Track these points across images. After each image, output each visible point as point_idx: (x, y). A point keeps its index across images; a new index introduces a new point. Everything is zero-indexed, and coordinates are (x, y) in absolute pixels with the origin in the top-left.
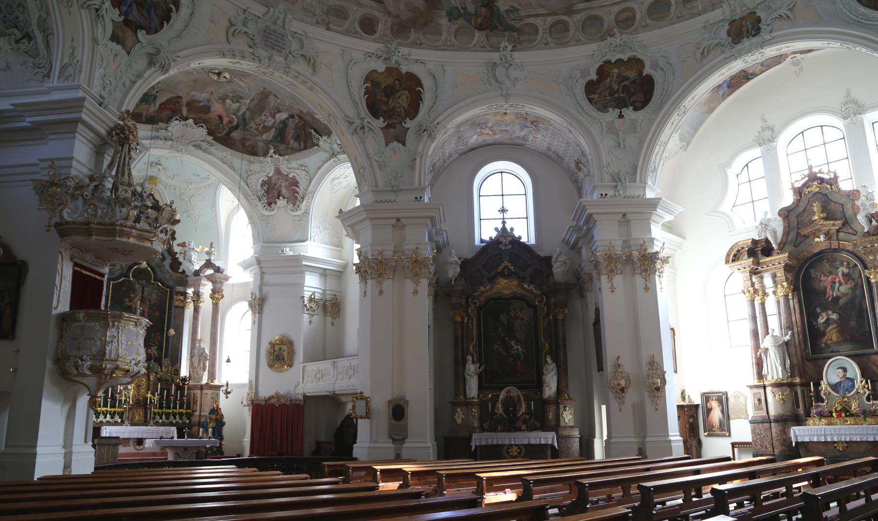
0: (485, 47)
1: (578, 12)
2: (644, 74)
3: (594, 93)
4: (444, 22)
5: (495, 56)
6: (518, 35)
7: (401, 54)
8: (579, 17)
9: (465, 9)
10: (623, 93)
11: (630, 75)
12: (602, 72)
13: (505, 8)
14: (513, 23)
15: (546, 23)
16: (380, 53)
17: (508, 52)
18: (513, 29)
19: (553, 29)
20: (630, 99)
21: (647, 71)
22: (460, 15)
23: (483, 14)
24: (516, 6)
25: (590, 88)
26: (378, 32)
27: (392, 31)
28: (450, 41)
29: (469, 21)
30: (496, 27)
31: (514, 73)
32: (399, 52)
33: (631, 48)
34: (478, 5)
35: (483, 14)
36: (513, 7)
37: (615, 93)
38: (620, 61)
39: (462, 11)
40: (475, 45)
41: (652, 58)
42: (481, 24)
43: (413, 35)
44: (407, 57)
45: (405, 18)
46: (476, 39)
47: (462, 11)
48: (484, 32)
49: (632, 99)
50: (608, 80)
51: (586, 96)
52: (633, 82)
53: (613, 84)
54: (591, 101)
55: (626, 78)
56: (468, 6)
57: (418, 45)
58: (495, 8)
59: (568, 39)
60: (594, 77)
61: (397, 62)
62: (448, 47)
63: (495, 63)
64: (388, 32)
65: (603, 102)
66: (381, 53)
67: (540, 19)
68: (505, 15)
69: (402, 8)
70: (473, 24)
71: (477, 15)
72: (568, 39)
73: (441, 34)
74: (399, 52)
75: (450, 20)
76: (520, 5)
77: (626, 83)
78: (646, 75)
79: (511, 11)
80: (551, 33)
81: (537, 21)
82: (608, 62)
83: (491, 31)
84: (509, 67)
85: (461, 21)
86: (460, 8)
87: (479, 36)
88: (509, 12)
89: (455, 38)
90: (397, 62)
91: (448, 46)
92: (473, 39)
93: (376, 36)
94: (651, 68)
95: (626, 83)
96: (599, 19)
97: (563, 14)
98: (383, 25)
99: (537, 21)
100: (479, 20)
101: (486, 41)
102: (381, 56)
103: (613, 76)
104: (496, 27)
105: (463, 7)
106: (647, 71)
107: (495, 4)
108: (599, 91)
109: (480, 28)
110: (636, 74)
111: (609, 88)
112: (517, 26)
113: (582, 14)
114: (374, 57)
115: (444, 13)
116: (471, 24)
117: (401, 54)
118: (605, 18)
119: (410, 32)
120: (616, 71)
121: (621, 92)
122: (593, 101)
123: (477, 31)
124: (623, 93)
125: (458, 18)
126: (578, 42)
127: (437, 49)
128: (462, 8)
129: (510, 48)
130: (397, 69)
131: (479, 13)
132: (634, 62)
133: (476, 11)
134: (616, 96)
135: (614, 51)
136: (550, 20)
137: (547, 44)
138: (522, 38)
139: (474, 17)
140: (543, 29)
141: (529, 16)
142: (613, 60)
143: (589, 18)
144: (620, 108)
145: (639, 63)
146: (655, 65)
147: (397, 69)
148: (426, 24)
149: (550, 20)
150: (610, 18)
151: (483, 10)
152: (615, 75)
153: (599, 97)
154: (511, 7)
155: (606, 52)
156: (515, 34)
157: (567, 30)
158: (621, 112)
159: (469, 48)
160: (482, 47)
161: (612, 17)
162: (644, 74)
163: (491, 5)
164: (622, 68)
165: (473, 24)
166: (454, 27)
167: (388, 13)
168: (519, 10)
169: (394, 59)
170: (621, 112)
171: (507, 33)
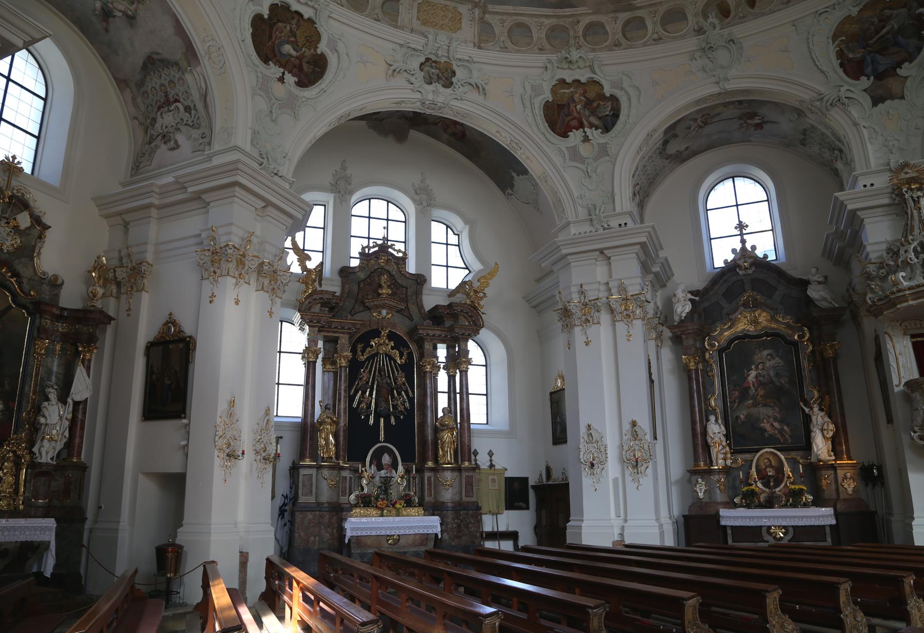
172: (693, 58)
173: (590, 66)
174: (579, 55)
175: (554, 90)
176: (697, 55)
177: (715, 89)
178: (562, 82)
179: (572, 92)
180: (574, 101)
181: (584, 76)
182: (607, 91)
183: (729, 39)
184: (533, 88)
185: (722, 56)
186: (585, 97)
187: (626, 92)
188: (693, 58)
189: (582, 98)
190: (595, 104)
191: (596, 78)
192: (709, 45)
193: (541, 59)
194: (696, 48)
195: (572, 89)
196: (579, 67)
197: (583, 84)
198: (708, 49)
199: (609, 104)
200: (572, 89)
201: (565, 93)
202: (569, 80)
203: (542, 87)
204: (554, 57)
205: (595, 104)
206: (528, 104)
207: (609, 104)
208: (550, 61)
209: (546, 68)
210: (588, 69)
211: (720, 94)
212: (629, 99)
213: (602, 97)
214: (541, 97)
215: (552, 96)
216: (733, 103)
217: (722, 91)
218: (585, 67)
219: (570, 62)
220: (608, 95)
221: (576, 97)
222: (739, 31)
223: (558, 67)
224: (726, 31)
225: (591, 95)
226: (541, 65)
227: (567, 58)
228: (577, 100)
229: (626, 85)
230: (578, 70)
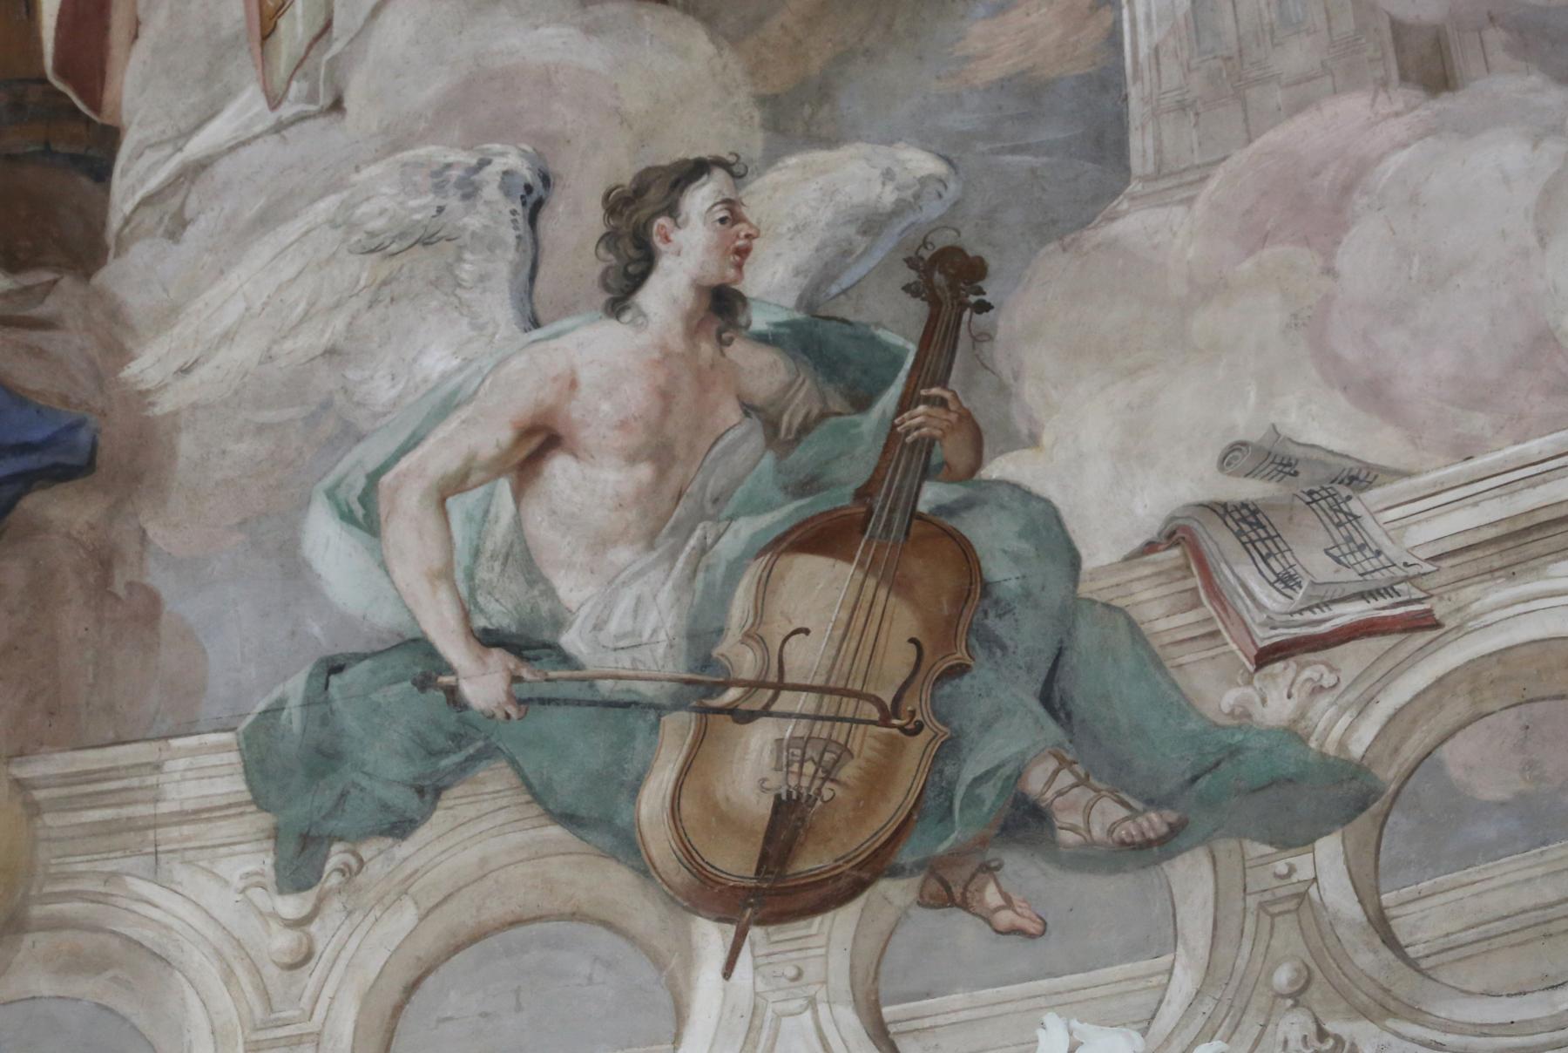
6: (1366, 886)
23: (806, 659)
34: (745, 531)
35: (806, 659)
56: (573, 589)
70: (659, 843)
86: (454, 649)
88: (1220, 541)
105: (498, 613)
107: (997, 468)
123: (711, 937)
125: (430, 792)
128: (489, 639)
131: (747, 663)
139: (677, 729)
154: (1234, 456)
163: (932, 495)
165: (659, 843)
168: (1359, 478)
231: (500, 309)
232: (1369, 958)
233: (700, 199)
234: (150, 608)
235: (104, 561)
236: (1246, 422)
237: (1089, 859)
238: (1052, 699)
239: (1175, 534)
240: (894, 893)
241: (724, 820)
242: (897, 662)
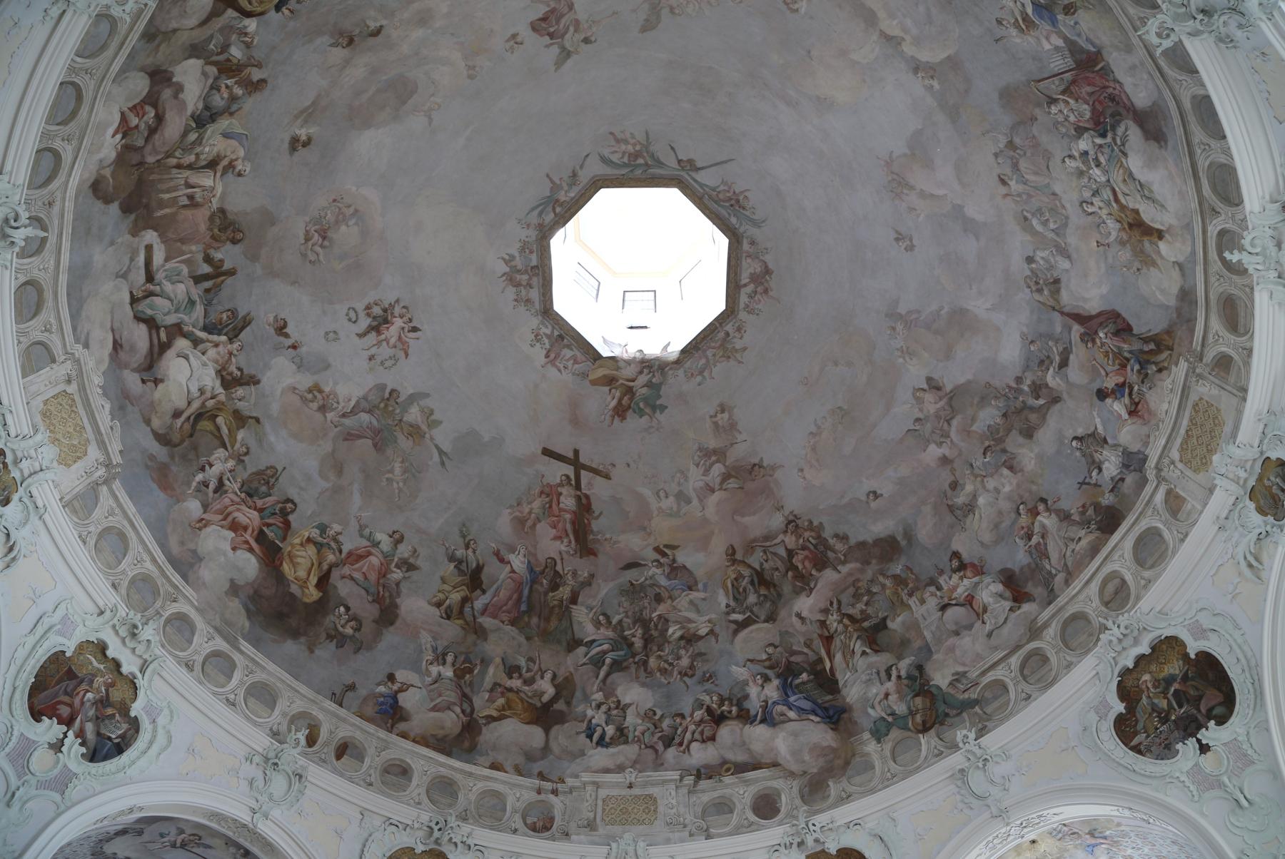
0: (942, 752)
1: (1046, 625)
2: (1193, 656)
3: (1136, 733)
4: (871, 747)
5: (956, 760)
7: (818, 826)
8: (1051, 632)
9: (893, 714)
10: (1180, 706)
11: (1172, 671)
12: (1127, 691)
13: (947, 682)
14: (966, 696)
15: (1012, 668)
16: (787, 840)
17: (972, 742)
18: (972, 703)
19: (1026, 672)
20: (1199, 711)
21: (1193, 648)
22: (889, 726)
23: (920, 707)
24: (961, 669)
25: (1125, 728)
26: (783, 810)
27: (802, 797)
28: (889, 771)
29: (906, 728)
30: (947, 715)
31: (998, 770)
32: (814, 825)
33: (1145, 629)
34: (909, 698)
35: (920, 707)
36: (957, 673)
37: (1168, 714)
38: (1140, 659)
39: (890, 719)
40: (926, 758)
41: (1186, 623)
42: (924, 722)
43: (834, 788)
44: (830, 826)
45: (815, 770)
46: (924, 747)
47: (890, 719)
48: (932, 732)
49: (1203, 710)
50: (1144, 700)
51: (1126, 745)
52: (1185, 678)
53: (1156, 701)
54: (1137, 750)
55: (1169, 680)
56: (895, 708)
57: (846, 798)
58: (933, 690)
59: (1053, 673)
60: (1120, 707)
61: (817, 841)
62: (890, 780)
63: (962, 771)
64: (798, 801)
65: (1157, 740)
66: (790, 839)
67: (1000, 667)
68: (952, 691)
69: (807, 758)
71: (912, 713)
72: (1053, 673)
73: (873, 768)
74: (814, 825)
75: (879, 741)
76: (964, 665)
77: (1175, 686)
78: (1197, 655)
79: (957, 680)
80: (1025, 678)
81: (998, 674)
82: (1125, 673)
83: (942, 724)
84: (984, 765)
85: (895, 734)
87: (927, 742)
89: (895, 762)
90: (817, 841)
91: (888, 780)
92: (920, 750)
93: (781, 816)
94: (1196, 640)
95: (1175, 686)
96: (1079, 617)
97: (1028, 642)
98: (788, 793)
99: (998, 674)
100: (919, 718)
101: (940, 742)
102: (791, 844)
103: (1148, 688)
104: (947, 715)
105: (889, 712)
106: (1193, 648)
108: (1140, 726)
109: (925, 729)
110: (1181, 662)
111: (1153, 710)
112: (974, 695)
113: (1054, 625)
114: (782, 849)
115: (866, 735)
116: (909, 730)
117: (818, 826)
118: (1088, 610)
119: (828, 786)
120: (1146, 677)
121: (1176, 707)
122: (1142, 747)
123: (921, 736)
124: (1180, 706)
125: (889, 731)
126: (1069, 666)
127: (873, 791)
129: (972, 735)
130: (823, 851)
132: (1164, 647)
133: (909, 708)
134: (1173, 718)
135: (1124, 649)
136: (1015, 661)
137: (1029, 697)
138: (989, 710)
139: (910, 717)
140: (1012, 680)
141: (984, 673)
142: (1131, 665)
143: (1066, 624)
144: (1193, 735)
145: (1173, 643)
146: (1200, 632)
147: (823, 851)
148: (847, 763)
149: (1015, 661)
150: (1094, 605)
151: (919, 700)
152: (1150, 685)
153: (1148, 737)
154: (953, 675)
155: (1114, 658)
156: (977, 709)
157: (1045, 660)
158: (1199, 741)
159: (919, 767)
160: (937, 756)
161: (1096, 602)
162: (1193, 656)
164: (1153, 667)
166: (888, 747)
167: (792, 774)
168: (966, 672)
169: (810, 841)
170: (1199, 741)
171: (965, 714)
172: (249, 759)
173: (146, 661)
174: (149, 638)
175: (81, 647)
176: (257, 759)
177: (245, 817)
178: (102, 648)
179: (99, 670)
180: (91, 682)
181: (129, 666)
182: (136, 709)
183: (299, 771)
184: (65, 618)
185: (279, 783)
186: (107, 691)
187: (155, 731)
188: (249, 759)
189: (103, 689)
190: (110, 711)
191: (140, 682)
192: (277, 761)
193: (110, 598)
194: (261, 750)
195: (102, 667)
196: (134, 649)
197: (121, 674)
198: (271, 763)
199: (125, 726)
200: (102, 667)
201: (91, 663)
202: (110, 653)
203: (74, 630)
204: (122, 611)
205: (110, 711)
206: (40, 630)
207: (125, 726)
208: (114, 610)
209: (102, 613)
210: (140, 662)
211: (244, 826)
212: (151, 743)
213: (124, 710)
214: (61, 640)
215: (74, 652)
216: (238, 846)
217: (251, 826)
218: (140, 657)
219: (134, 635)
220: (133, 714)
221: (99, 680)
222: (319, 775)
223: (114, 626)
224: (302, 761)
225: (116, 695)
226: (101, 604)
227: (135, 627)
228: (95, 685)
229: (161, 721)
230: (128, 652)
231: (878, 684)
232: (985, 716)
233: (894, 668)
234: (856, 722)
235: (850, 719)
236: (953, 671)
237: (954, 716)
238: (945, 703)
239: (950, 684)
240: (937, 726)
241: (918, 724)
242: (928, 704)
